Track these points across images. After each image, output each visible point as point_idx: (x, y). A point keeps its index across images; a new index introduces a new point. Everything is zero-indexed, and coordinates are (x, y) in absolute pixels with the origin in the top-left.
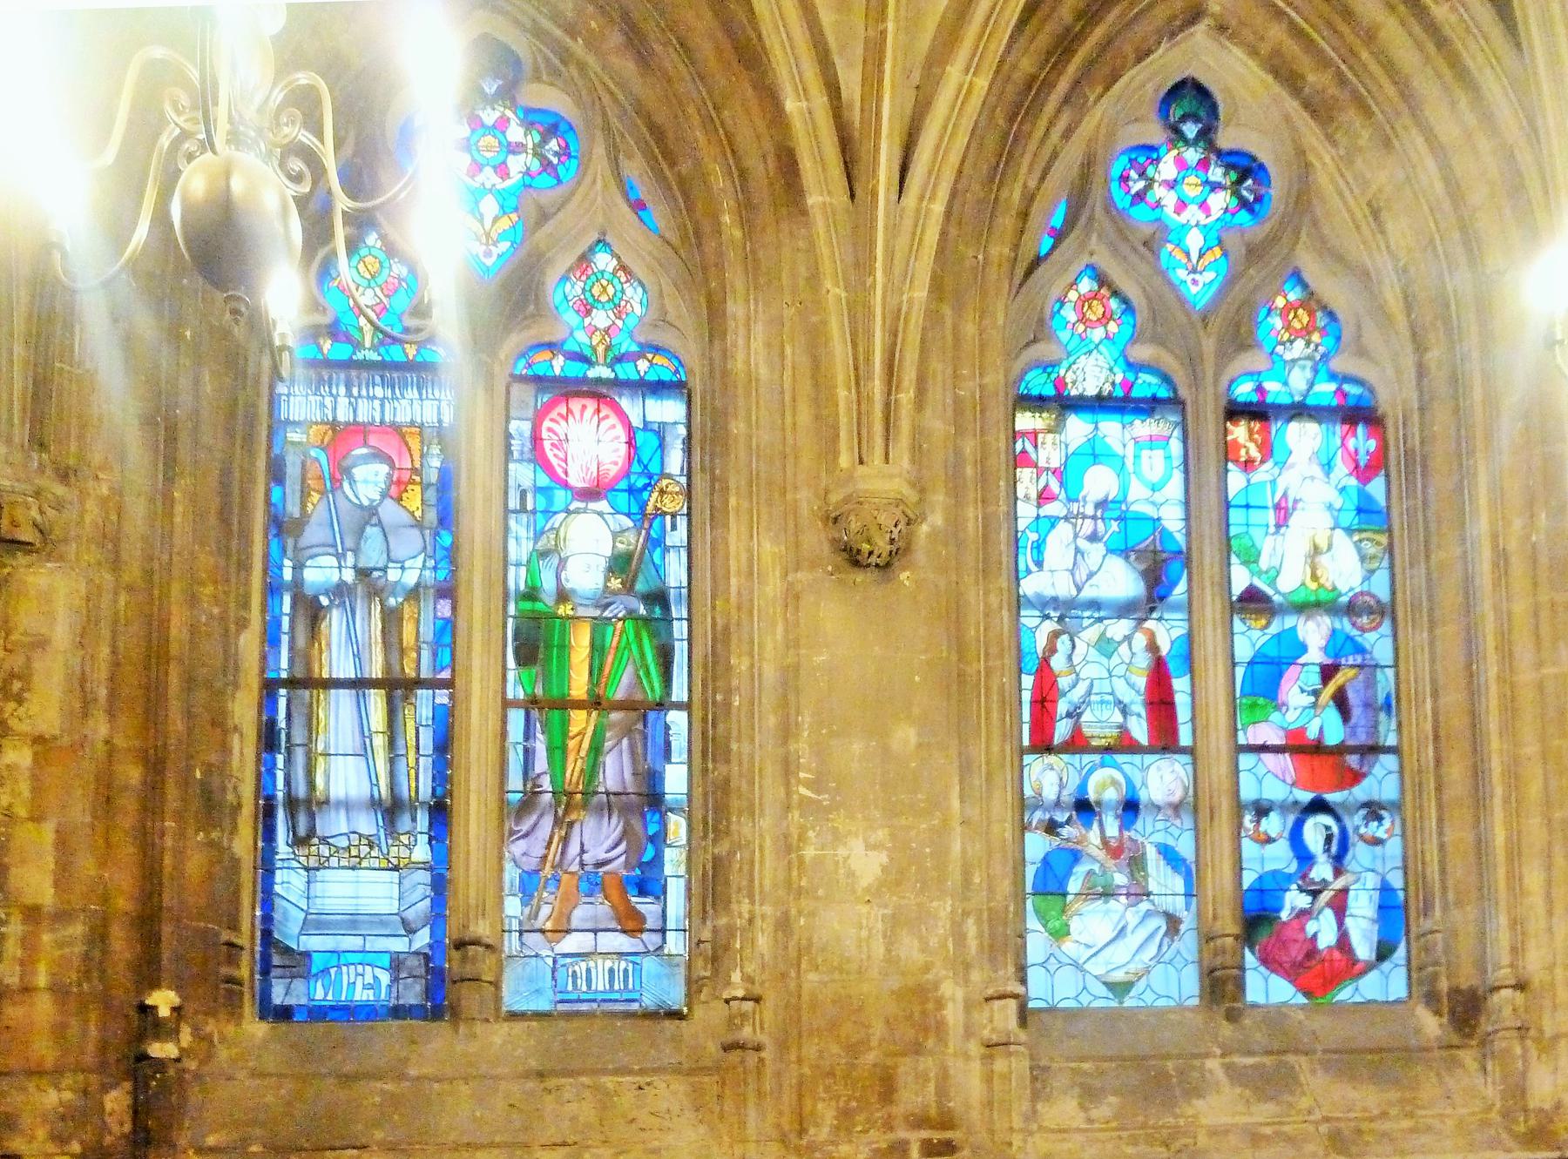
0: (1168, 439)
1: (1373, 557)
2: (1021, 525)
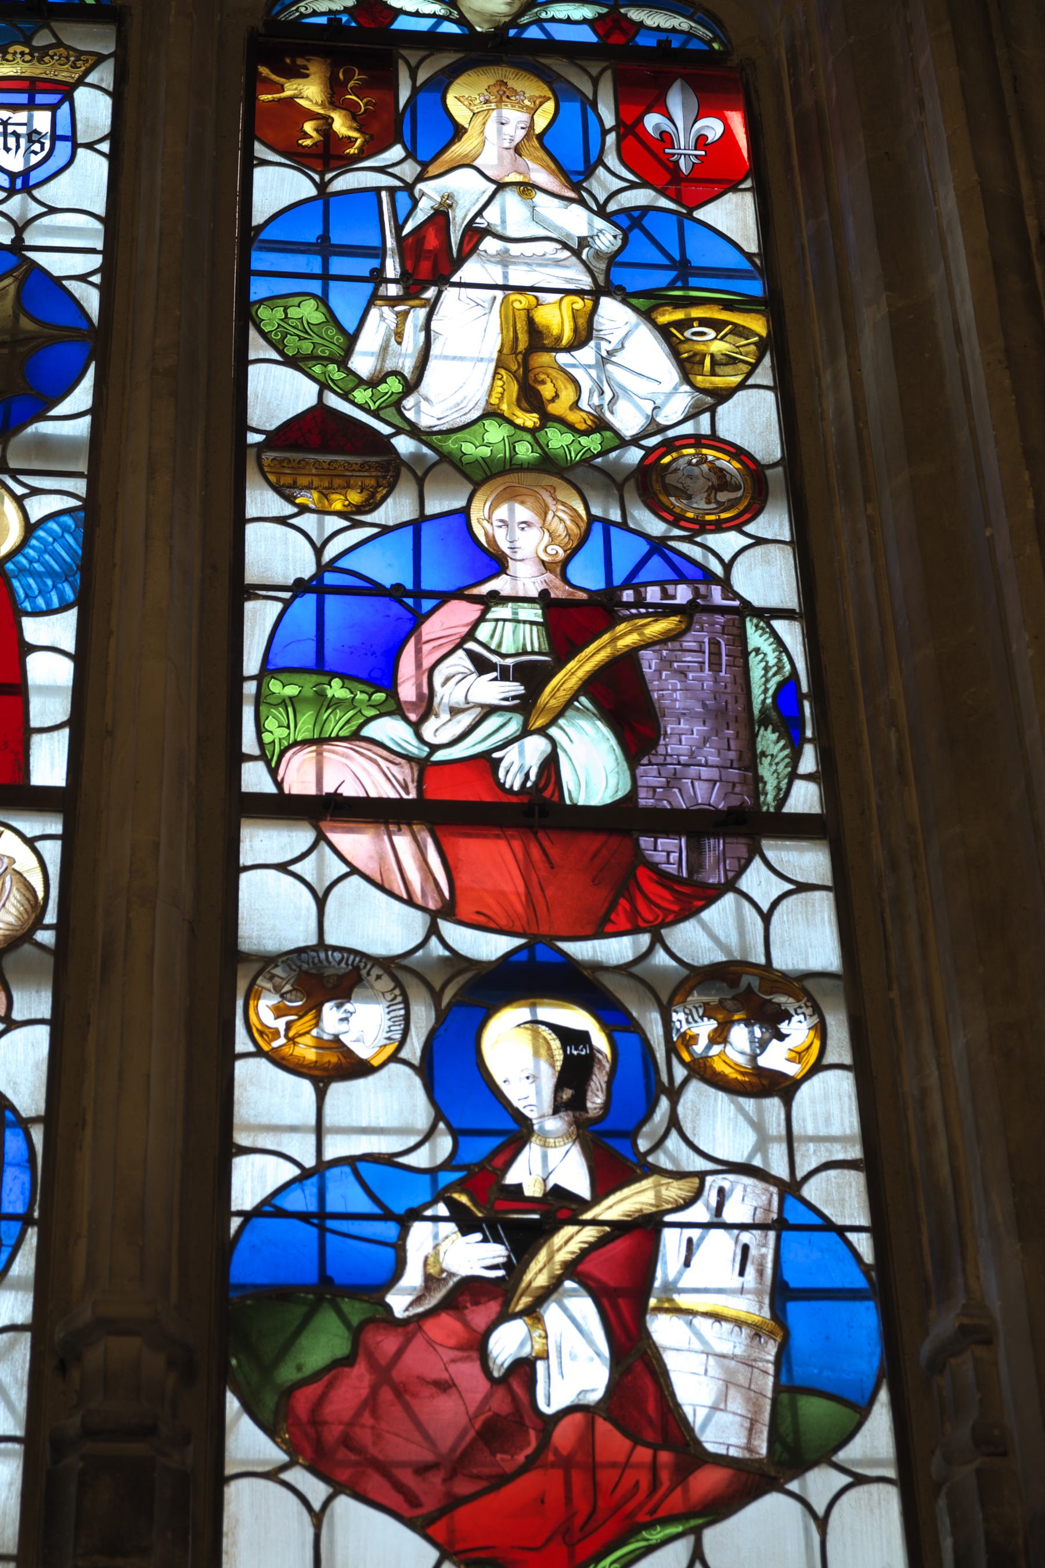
0: (66, 92)
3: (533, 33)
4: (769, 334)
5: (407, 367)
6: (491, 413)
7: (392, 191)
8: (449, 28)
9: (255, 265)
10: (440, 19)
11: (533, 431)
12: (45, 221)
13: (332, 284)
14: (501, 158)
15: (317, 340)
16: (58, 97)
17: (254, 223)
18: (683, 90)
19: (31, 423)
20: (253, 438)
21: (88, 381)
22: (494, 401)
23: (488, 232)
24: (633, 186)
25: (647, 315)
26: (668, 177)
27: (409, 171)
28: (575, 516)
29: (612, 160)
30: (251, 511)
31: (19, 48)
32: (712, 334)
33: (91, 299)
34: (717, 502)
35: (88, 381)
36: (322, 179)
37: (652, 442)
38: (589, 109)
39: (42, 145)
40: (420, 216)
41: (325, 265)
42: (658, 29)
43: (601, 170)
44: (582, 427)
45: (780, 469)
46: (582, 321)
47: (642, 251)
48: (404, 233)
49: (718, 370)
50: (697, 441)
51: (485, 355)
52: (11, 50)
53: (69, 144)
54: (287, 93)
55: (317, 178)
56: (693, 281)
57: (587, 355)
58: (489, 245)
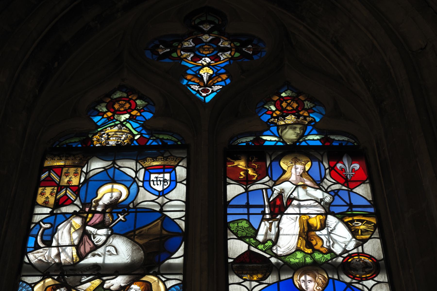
1: (364, 232)
2: (37, 219)
3: (304, 144)
4: (377, 222)
5: (273, 238)
6: (298, 249)
7: (266, 189)
8: (280, 144)
9: (228, 212)
10: (277, 142)
11: (310, 254)
12: (169, 203)
13: (250, 216)
14: (296, 178)
15: (247, 232)
16: (172, 169)
17: (228, 200)
18: (347, 157)
19: (166, 260)
20: (230, 261)
21: (182, 247)
22: (299, 246)
23: (294, 199)
24: (335, 184)
25: (341, 220)
26: (344, 181)
27: (270, 183)
28: (324, 278)
29: (328, 177)
30: (230, 281)
31: (160, 157)
32: (361, 224)
33: (182, 224)
34: (365, 272)
35: (182, 247)
36: (246, 187)
37: (345, 255)
38: (321, 163)
39: (167, 183)
40: (275, 196)
41: (248, 211)
42: (339, 140)
43: (325, 180)
44: (325, 252)
45: (383, 261)
46: (322, 222)
47: (338, 201)
48: (270, 200)
49: (363, 234)
50: (358, 254)
51: (295, 233)
52: (158, 158)
53: (175, 182)
54: (235, 164)
55: (245, 187)
56: (354, 209)
57: (324, 232)
58: (295, 202)
